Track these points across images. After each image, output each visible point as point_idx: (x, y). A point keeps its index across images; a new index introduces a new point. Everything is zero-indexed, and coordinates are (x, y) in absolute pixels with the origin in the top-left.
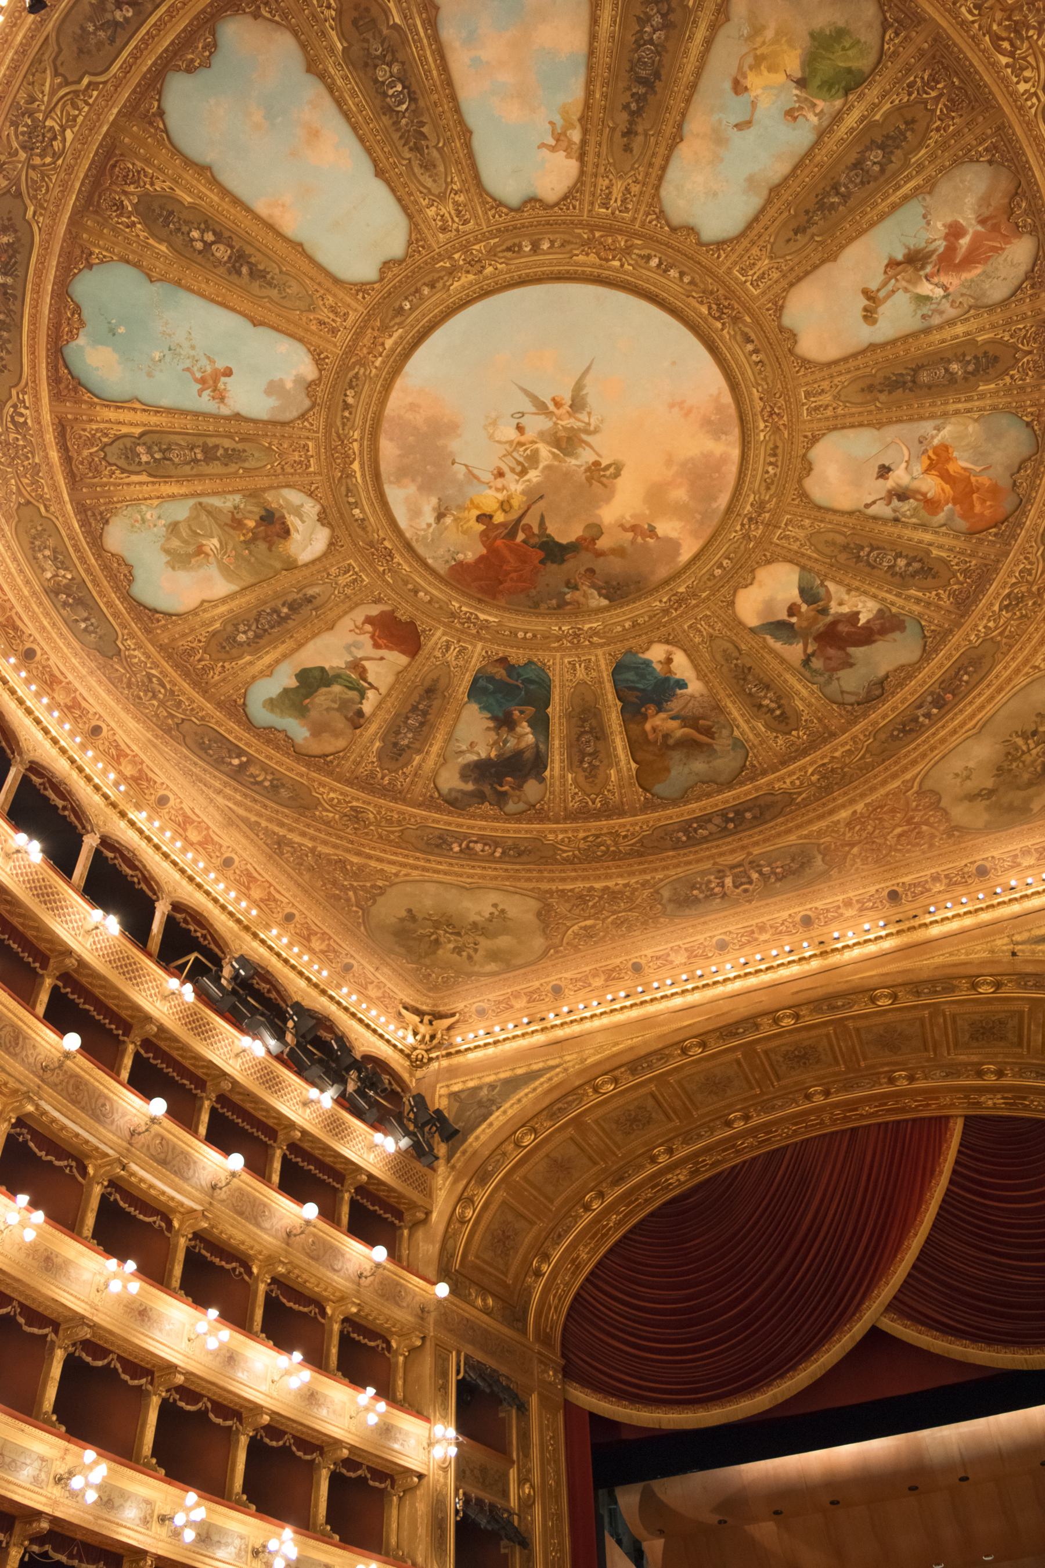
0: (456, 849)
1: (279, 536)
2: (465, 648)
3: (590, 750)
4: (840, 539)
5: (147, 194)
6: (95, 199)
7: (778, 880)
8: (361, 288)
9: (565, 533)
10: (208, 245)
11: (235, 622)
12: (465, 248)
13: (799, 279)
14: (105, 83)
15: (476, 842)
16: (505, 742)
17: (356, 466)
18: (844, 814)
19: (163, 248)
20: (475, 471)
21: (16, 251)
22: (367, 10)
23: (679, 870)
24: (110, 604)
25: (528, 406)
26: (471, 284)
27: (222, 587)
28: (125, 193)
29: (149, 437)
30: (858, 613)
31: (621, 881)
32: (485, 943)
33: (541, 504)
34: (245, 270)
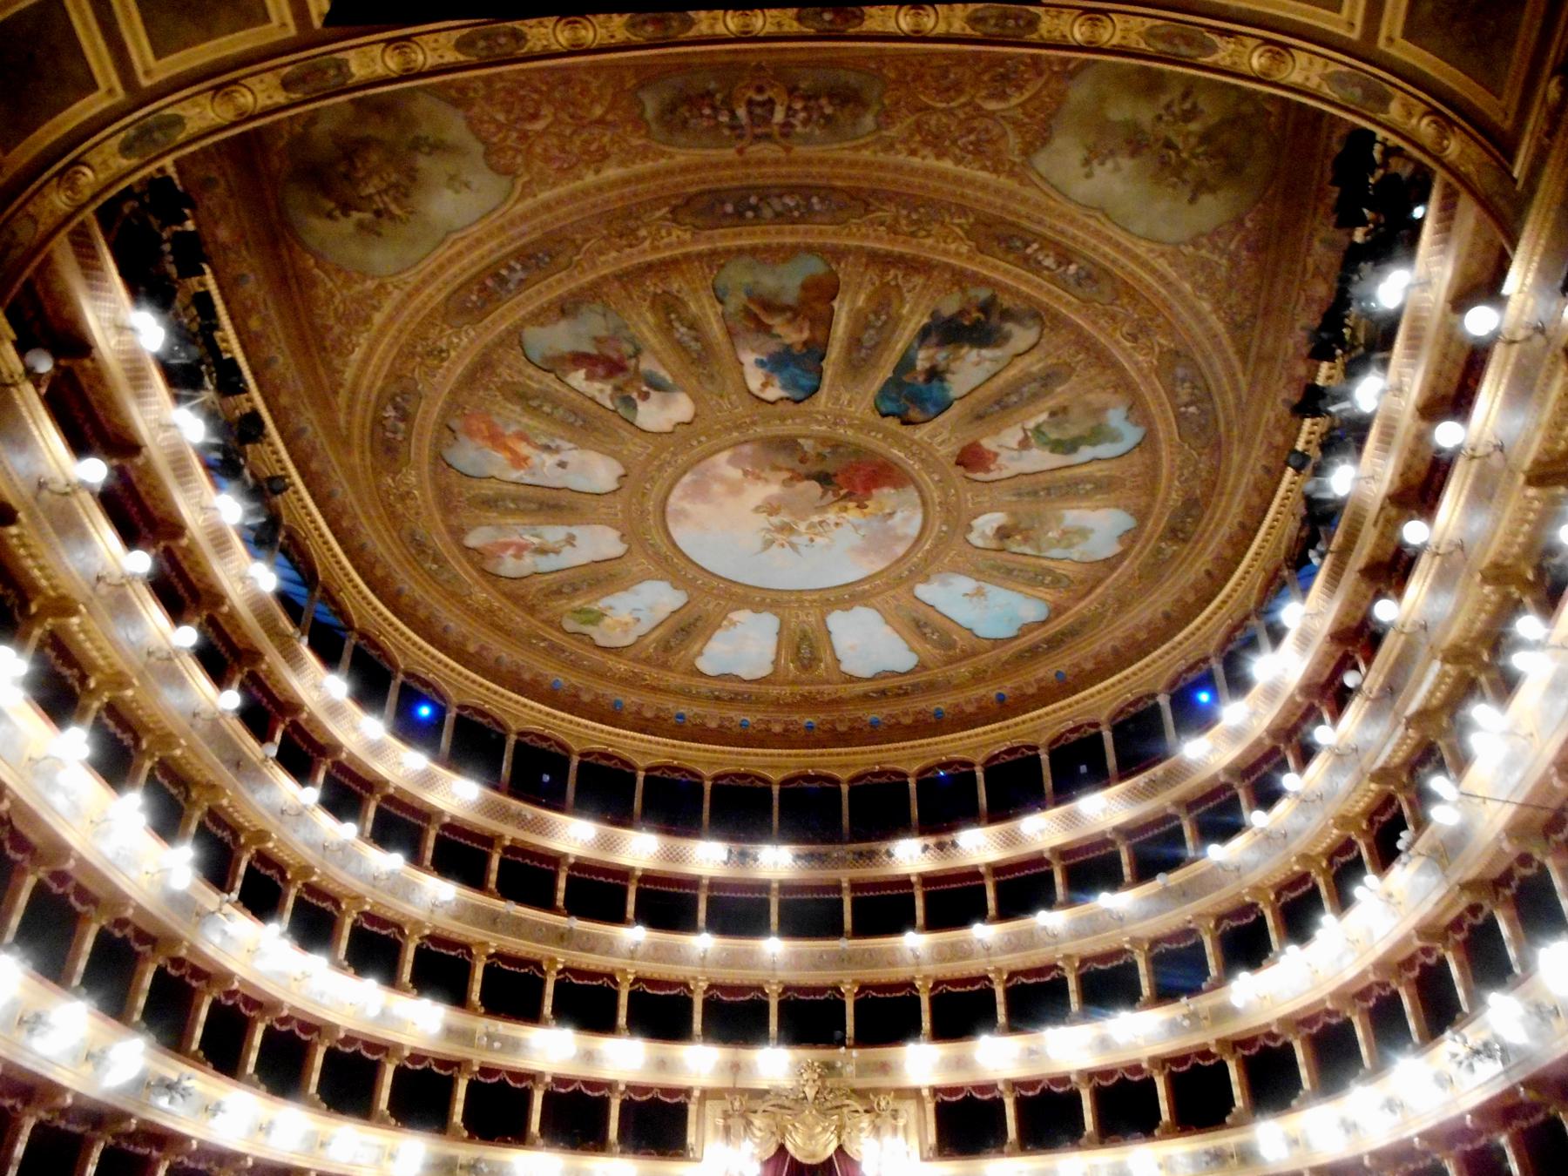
3: (872, 332)
7: (709, 94)
11: (1087, 495)
15: (1047, 268)
16: (946, 358)
18: (611, 172)
23: (836, 155)
25: (802, 549)
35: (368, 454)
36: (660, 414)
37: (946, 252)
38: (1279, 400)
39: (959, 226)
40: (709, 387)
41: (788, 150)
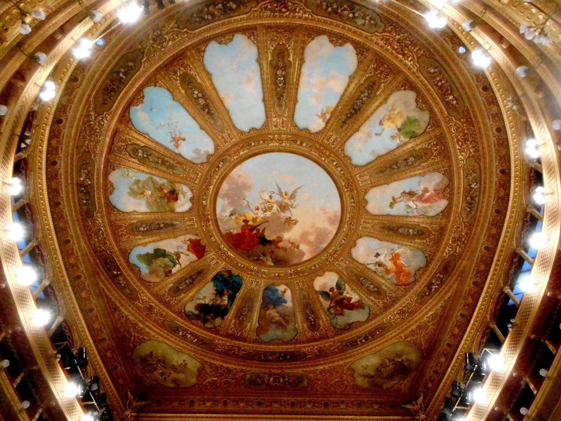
0: (181, 334)
1: (173, 199)
2: (219, 262)
4: (356, 272)
5: (187, 73)
6: (168, 66)
7: (289, 384)
8: (241, 132)
9: (270, 236)
10: (198, 97)
11: (142, 222)
12: (280, 135)
13: (376, 186)
14: (191, 34)
15: (189, 334)
16: (217, 300)
17: (212, 187)
18: (321, 368)
19: (183, 92)
20: (250, 205)
21: (132, 69)
22: (283, 52)
23: (256, 369)
24: (99, 198)
25: (276, 191)
26: (276, 146)
27: (143, 208)
28: (179, 69)
29: (145, 148)
30: (351, 298)
31: (234, 367)
32: (174, 375)
33: (267, 224)
34: (206, 110)
35: (457, 266)
36: (327, 281)
37: (222, 340)
38: (83, 276)
39: (219, 348)
40: (306, 293)
41: (270, 371)
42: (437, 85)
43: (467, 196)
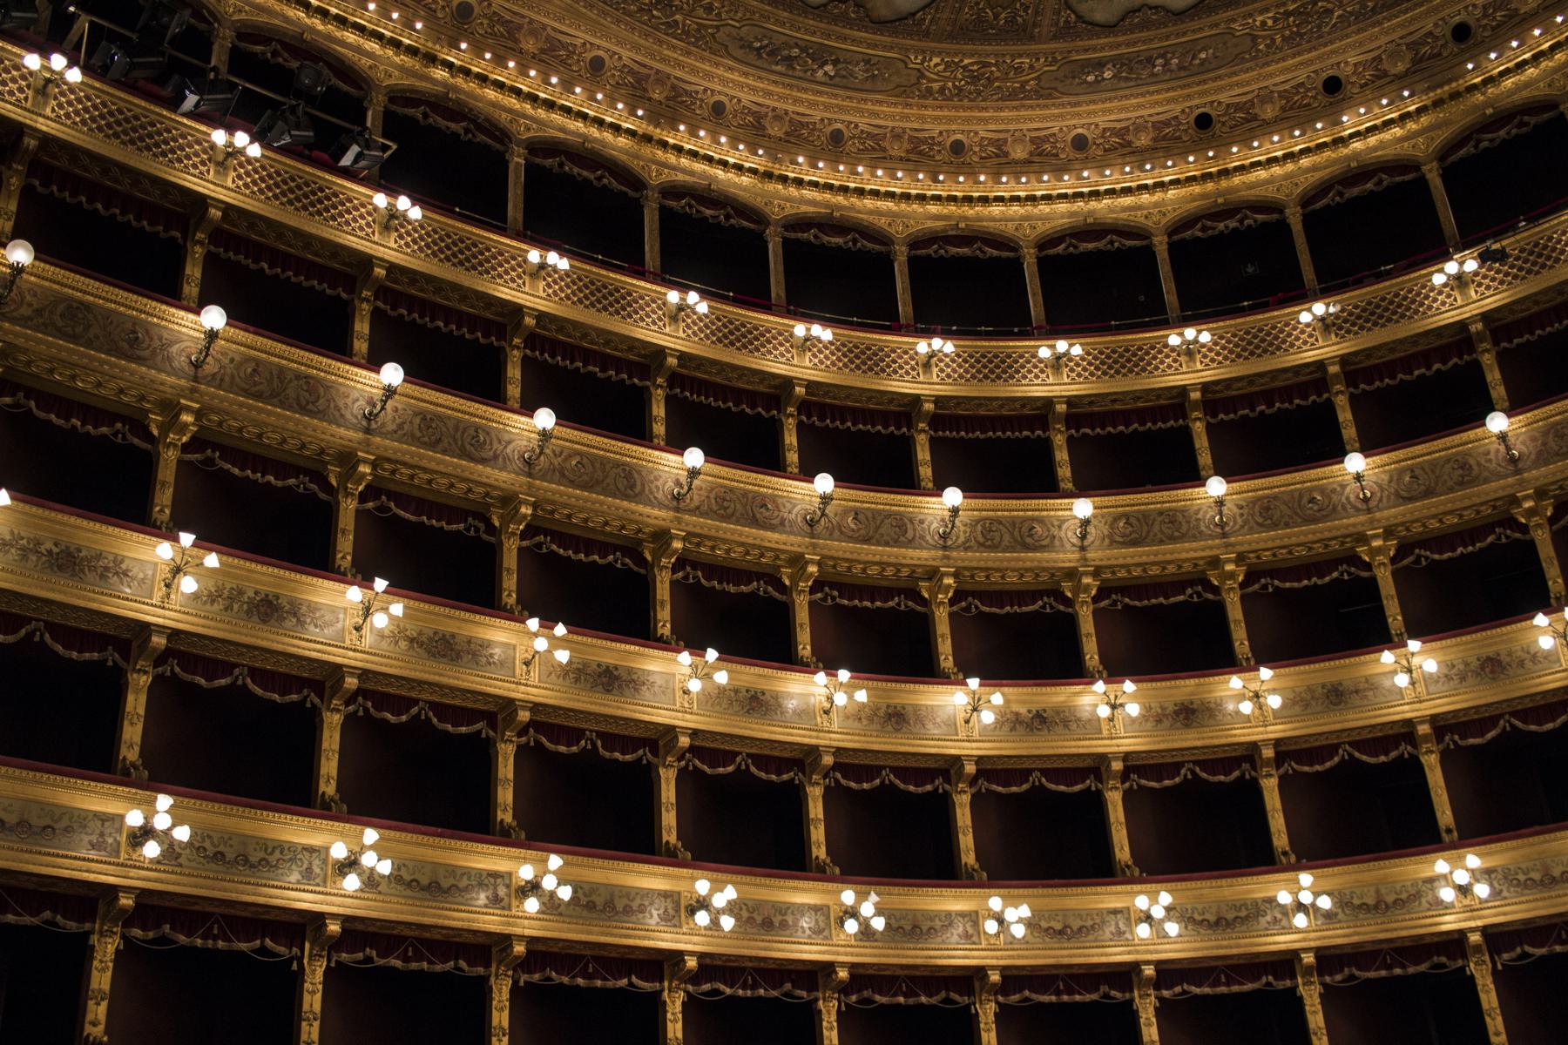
42: (1163, 56)
43: (802, 50)
